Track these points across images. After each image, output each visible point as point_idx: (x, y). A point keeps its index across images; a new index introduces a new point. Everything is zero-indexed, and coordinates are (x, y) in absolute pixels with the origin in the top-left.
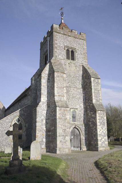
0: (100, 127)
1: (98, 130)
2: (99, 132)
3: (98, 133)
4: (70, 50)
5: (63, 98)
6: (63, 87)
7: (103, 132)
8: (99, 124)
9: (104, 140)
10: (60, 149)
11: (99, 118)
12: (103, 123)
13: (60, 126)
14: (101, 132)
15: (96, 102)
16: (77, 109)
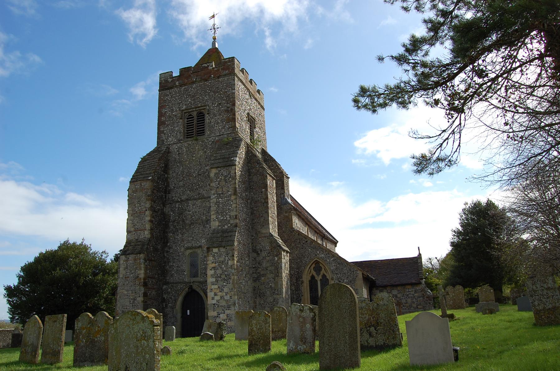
0: (216, 287)
1: (210, 294)
2: (213, 299)
3: (210, 302)
4: (195, 114)
5: (142, 234)
6: (144, 209)
7: (222, 297)
8: (214, 280)
9: (225, 317)
10: (401, 328)
11: (213, 265)
12: (223, 276)
13: (126, 292)
14: (217, 298)
15: (219, 226)
16: (200, 247)
